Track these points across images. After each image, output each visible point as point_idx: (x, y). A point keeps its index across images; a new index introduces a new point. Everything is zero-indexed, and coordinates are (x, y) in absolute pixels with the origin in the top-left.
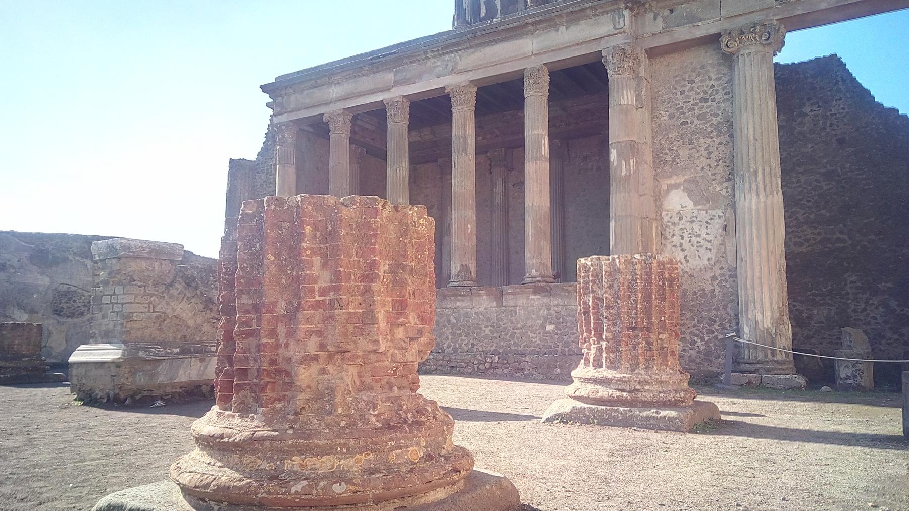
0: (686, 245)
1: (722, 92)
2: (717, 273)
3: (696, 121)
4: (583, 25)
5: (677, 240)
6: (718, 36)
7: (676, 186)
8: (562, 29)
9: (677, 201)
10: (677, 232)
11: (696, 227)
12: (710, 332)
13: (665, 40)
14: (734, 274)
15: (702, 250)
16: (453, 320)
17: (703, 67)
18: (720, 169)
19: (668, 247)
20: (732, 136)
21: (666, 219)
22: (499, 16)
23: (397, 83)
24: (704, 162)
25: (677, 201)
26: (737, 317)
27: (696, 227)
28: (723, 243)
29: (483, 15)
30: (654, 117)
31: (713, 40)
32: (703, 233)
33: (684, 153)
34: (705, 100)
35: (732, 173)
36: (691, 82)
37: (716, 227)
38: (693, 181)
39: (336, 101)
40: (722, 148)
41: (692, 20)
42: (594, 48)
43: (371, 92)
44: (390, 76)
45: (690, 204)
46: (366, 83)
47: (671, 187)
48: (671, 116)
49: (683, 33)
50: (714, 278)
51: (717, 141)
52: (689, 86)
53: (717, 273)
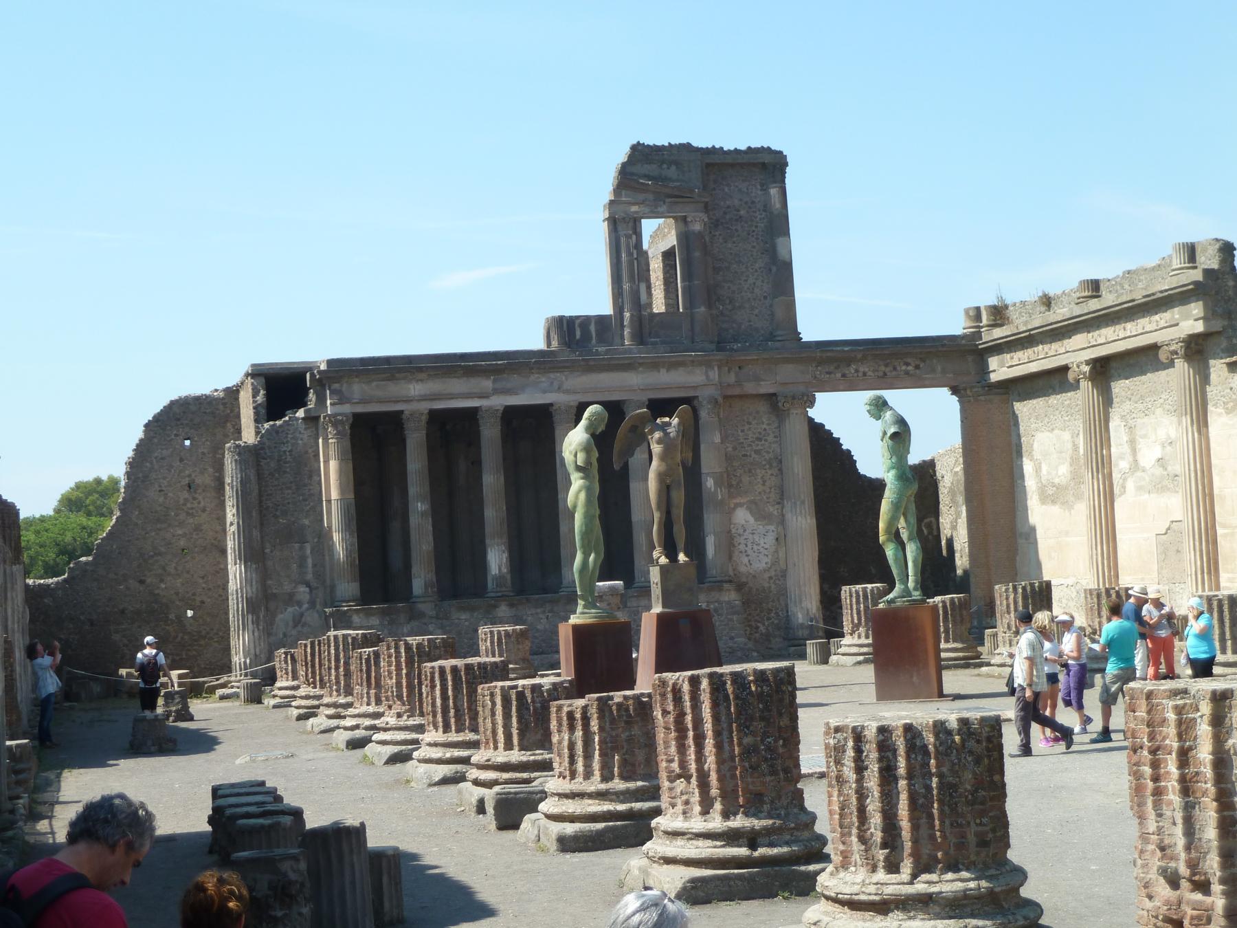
0: (749, 552)
1: (772, 435)
2: (773, 574)
3: (753, 455)
4: (681, 369)
5: (742, 547)
6: (775, 394)
7: (741, 505)
8: (663, 371)
9: (742, 516)
10: (743, 541)
11: (756, 537)
12: (769, 619)
13: (737, 391)
14: (784, 574)
15: (761, 556)
17: (758, 412)
19: (736, 553)
20: (780, 470)
21: (733, 531)
22: (594, 341)
23: (496, 391)
24: (759, 488)
25: (742, 516)
26: (787, 605)
27: (756, 537)
28: (776, 551)
29: (578, 334)
31: (771, 398)
32: (762, 542)
33: (746, 479)
34: (760, 440)
35: (782, 499)
36: (749, 423)
37: (770, 540)
38: (753, 502)
39: (416, 399)
40: (773, 478)
41: (757, 379)
42: (690, 394)
43: (459, 395)
44: (487, 384)
45: (752, 520)
46: (457, 385)
47: (737, 505)
48: (735, 449)
49: (750, 388)
50: (771, 578)
51: (770, 472)
52: (747, 427)
53: (773, 574)
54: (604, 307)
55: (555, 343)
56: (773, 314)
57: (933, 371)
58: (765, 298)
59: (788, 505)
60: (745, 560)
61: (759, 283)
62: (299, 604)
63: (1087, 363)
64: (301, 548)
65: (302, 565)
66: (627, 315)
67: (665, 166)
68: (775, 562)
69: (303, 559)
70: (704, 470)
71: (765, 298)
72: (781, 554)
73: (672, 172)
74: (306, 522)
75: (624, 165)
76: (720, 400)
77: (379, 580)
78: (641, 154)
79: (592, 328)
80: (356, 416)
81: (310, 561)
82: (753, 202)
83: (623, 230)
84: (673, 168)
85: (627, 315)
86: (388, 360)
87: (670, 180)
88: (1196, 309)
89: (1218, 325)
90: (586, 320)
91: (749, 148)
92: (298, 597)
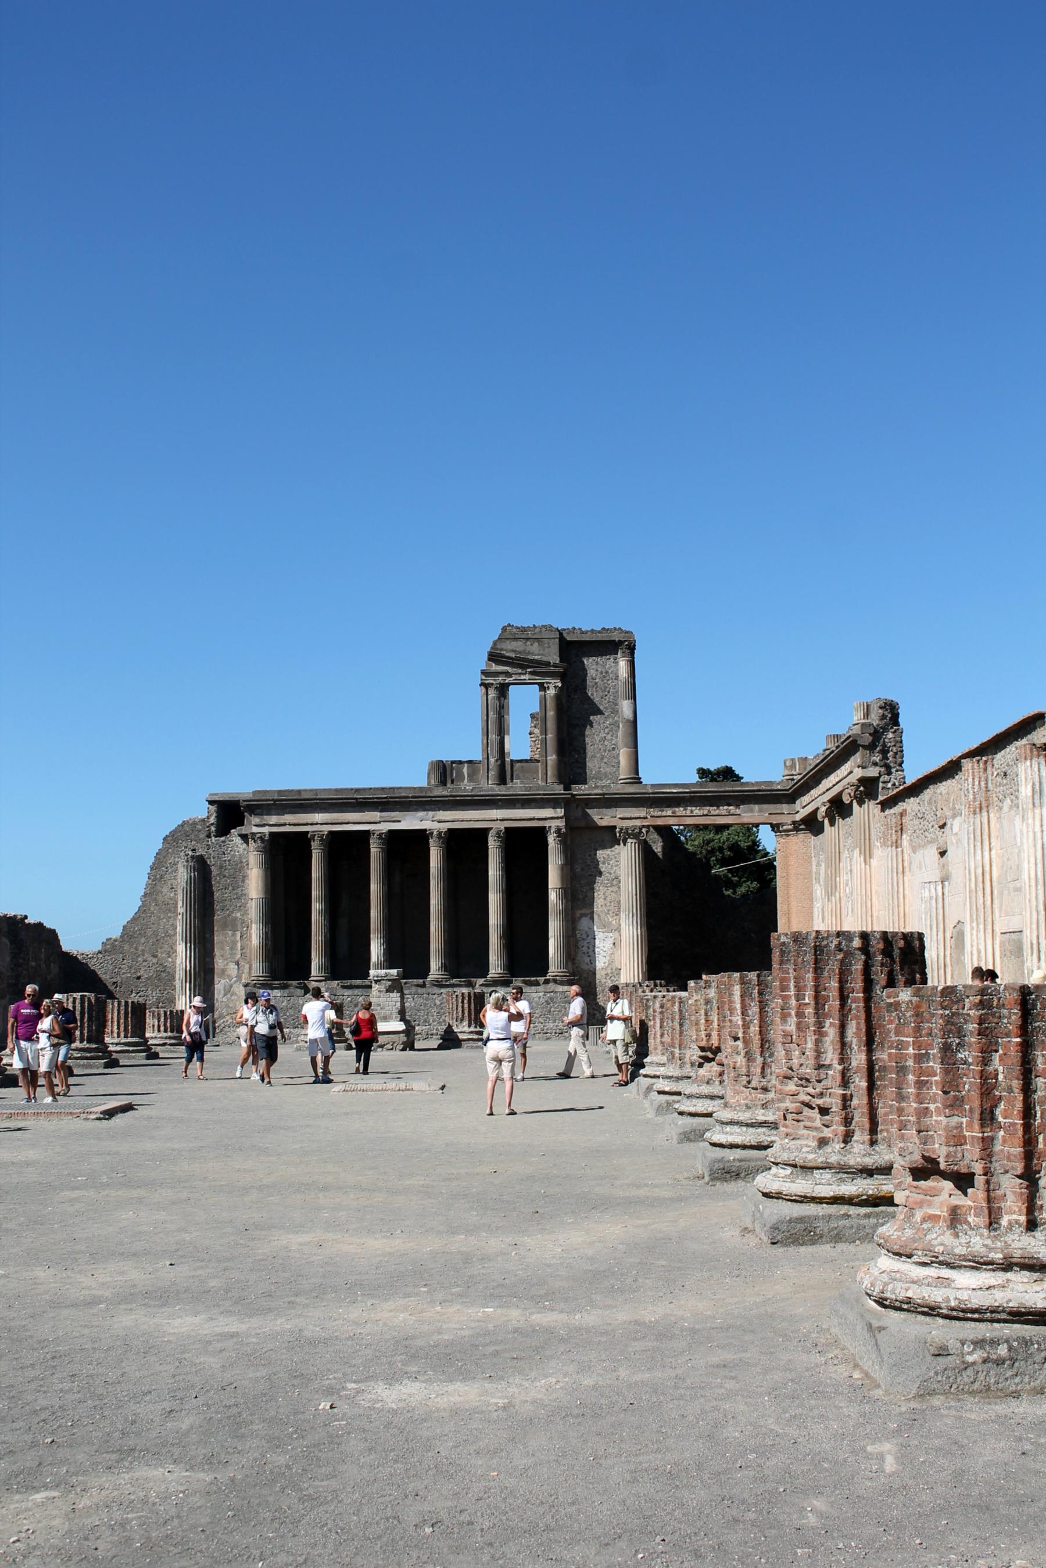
4: (533, 805)
5: (585, 949)
6: (615, 827)
10: (586, 945)
16: (438, 1003)
17: (603, 841)
18: (612, 908)
20: (619, 887)
21: (578, 936)
22: (466, 781)
30: (572, 869)
39: (319, 823)
43: (353, 821)
44: (376, 815)
47: (582, 915)
48: (582, 869)
53: (609, 971)
54: (477, 755)
55: (433, 782)
56: (619, 762)
57: (752, 811)
58: (614, 749)
59: (623, 915)
60: (587, 960)
61: (609, 737)
62: (230, 978)
63: (824, 804)
64: (234, 935)
65: (233, 948)
66: (492, 760)
67: (529, 643)
68: (611, 962)
69: (234, 943)
70: (550, 886)
71: (614, 749)
72: (616, 957)
73: (535, 648)
74: (239, 915)
75: (495, 643)
76: (564, 830)
77: (286, 964)
78: (508, 633)
79: (465, 770)
80: (271, 834)
81: (239, 945)
82: (607, 672)
83: (492, 693)
84: (536, 644)
85: (492, 760)
86: (299, 792)
87: (533, 654)
88: (857, 758)
89: (873, 772)
90: (460, 762)
91: (604, 629)
92: (229, 972)
